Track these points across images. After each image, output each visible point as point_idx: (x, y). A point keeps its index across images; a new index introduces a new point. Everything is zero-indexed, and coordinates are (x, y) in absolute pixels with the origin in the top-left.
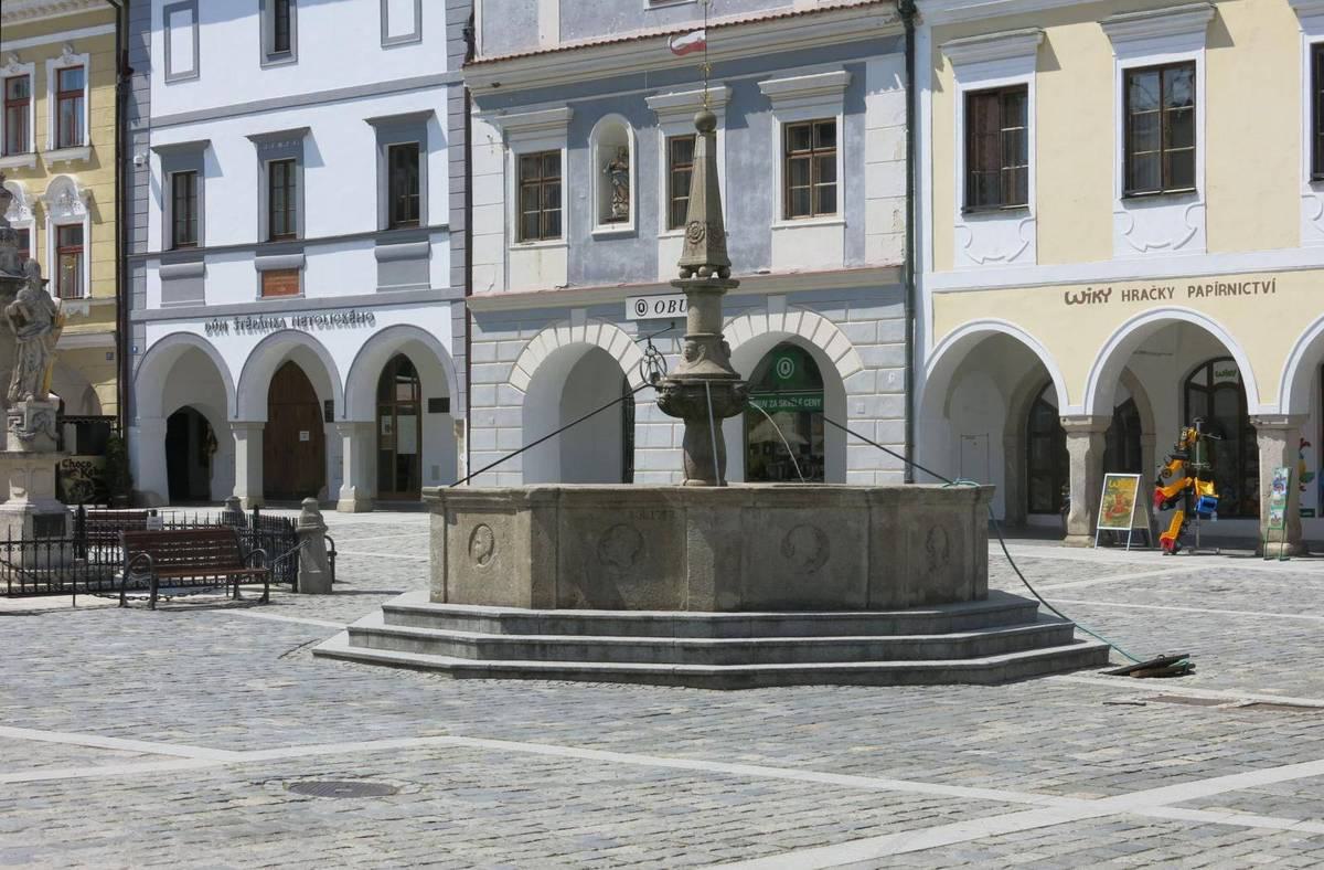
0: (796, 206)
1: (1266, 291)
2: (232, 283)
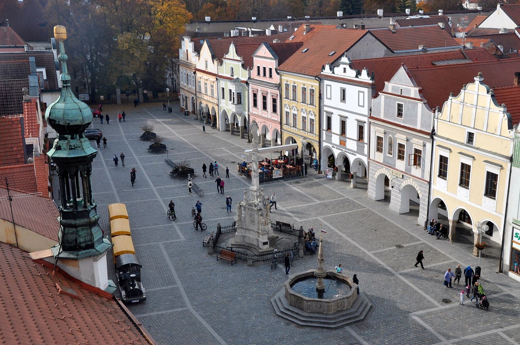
2: (336, 139)
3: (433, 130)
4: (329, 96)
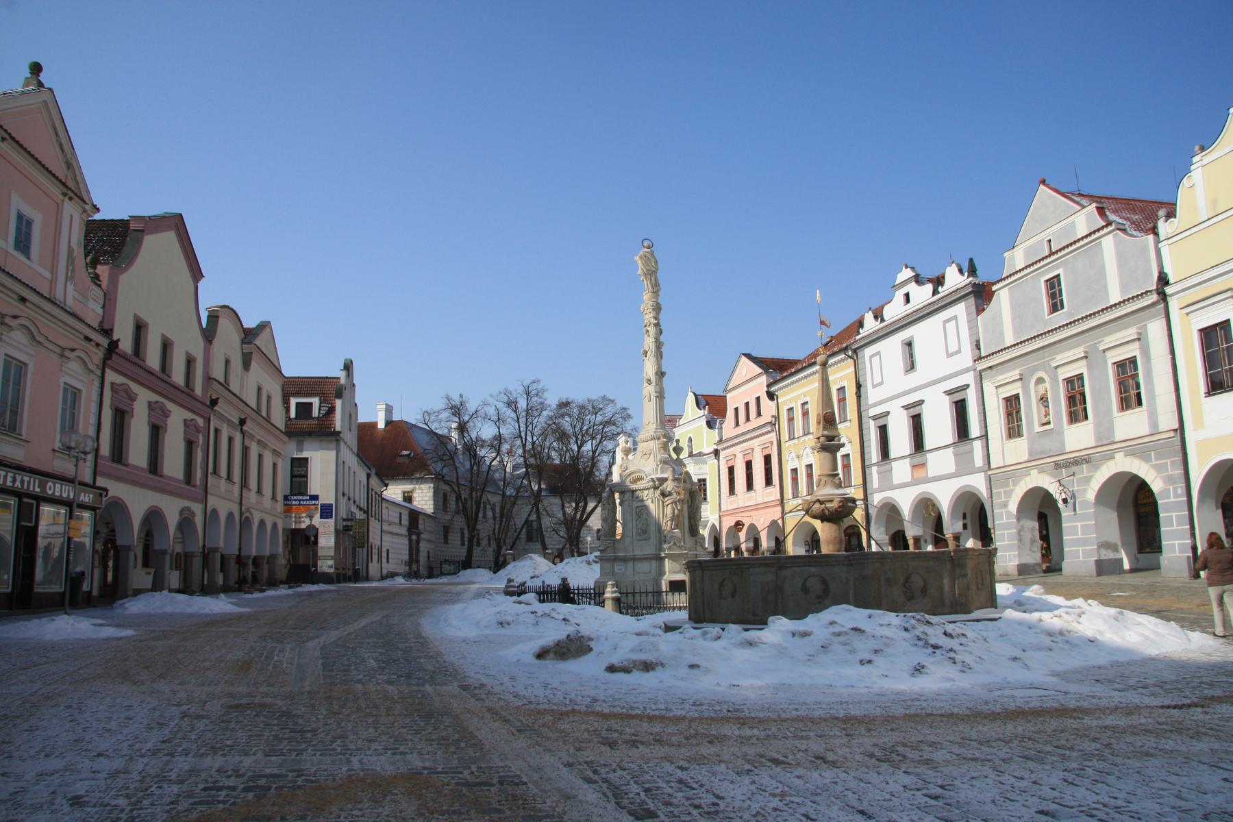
0: (1125, 404)
2: (901, 470)
3: (1163, 280)
4: (877, 380)
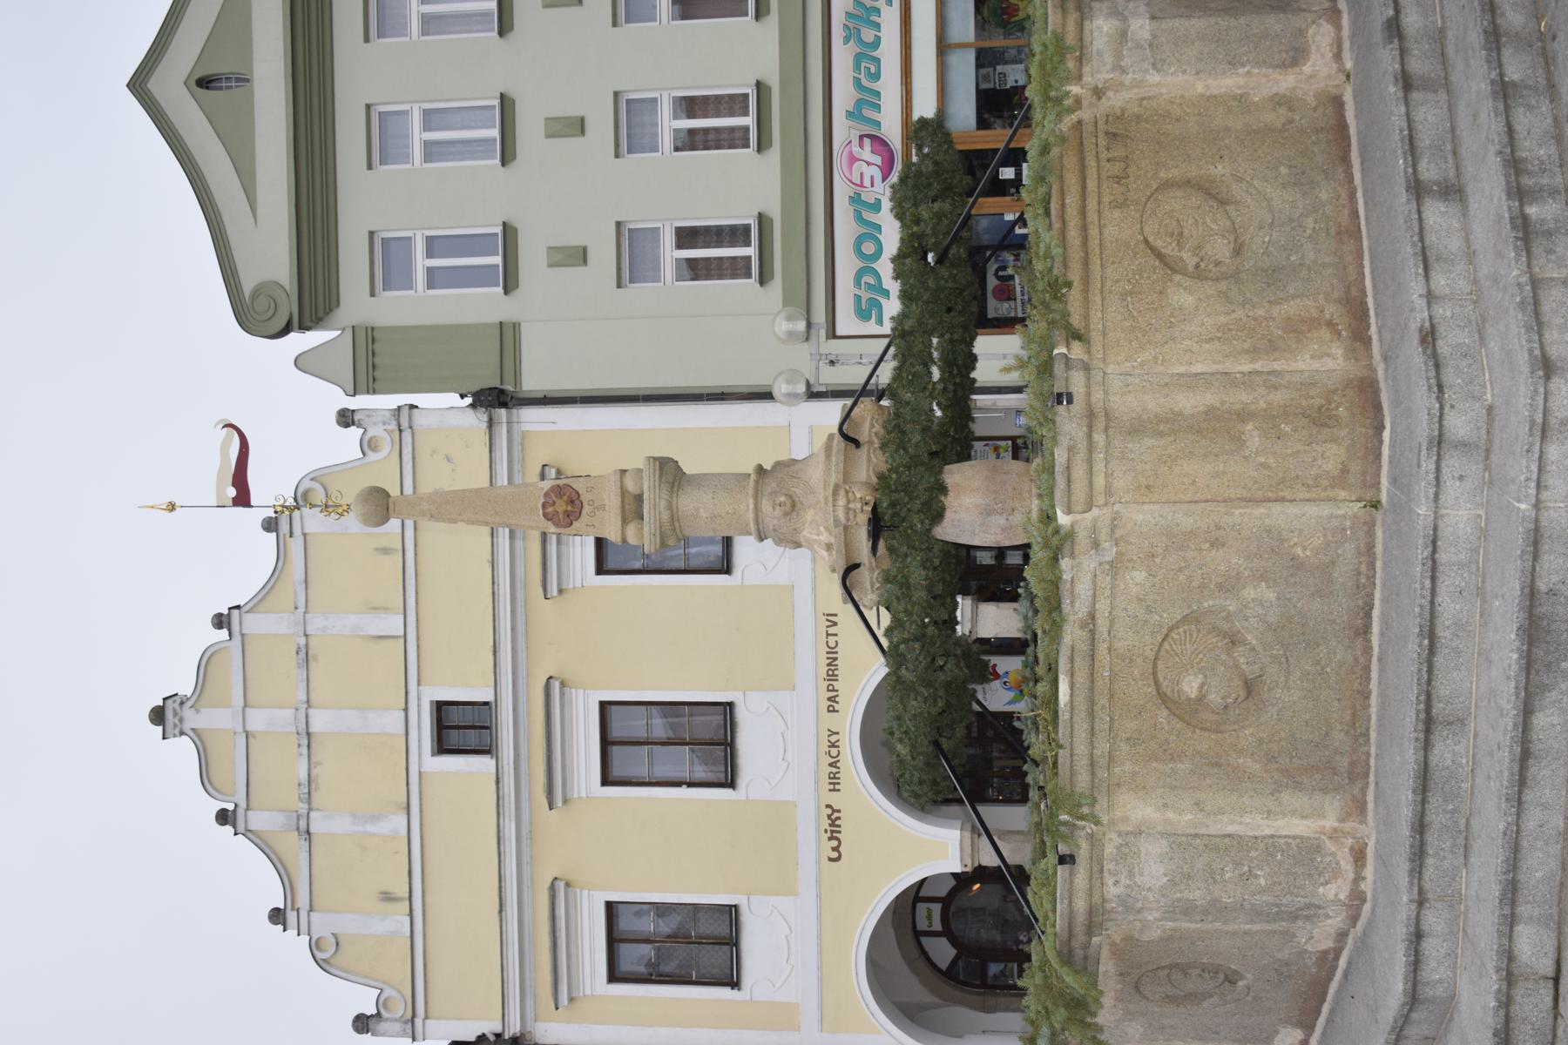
1: (835, 624)
